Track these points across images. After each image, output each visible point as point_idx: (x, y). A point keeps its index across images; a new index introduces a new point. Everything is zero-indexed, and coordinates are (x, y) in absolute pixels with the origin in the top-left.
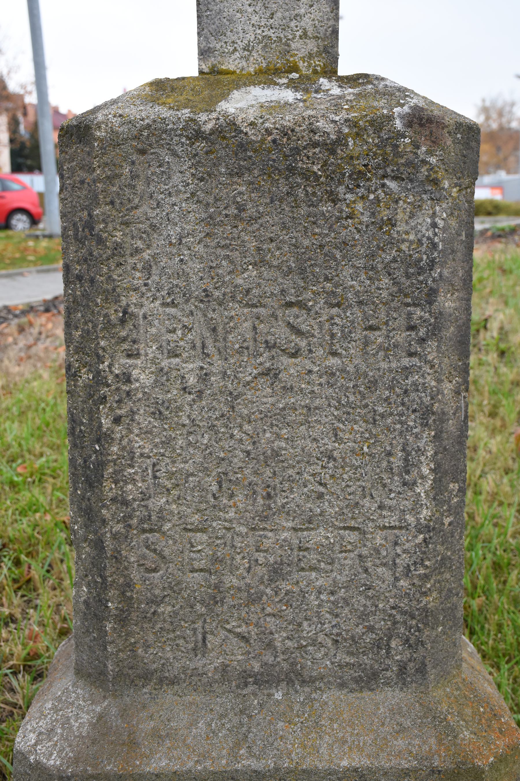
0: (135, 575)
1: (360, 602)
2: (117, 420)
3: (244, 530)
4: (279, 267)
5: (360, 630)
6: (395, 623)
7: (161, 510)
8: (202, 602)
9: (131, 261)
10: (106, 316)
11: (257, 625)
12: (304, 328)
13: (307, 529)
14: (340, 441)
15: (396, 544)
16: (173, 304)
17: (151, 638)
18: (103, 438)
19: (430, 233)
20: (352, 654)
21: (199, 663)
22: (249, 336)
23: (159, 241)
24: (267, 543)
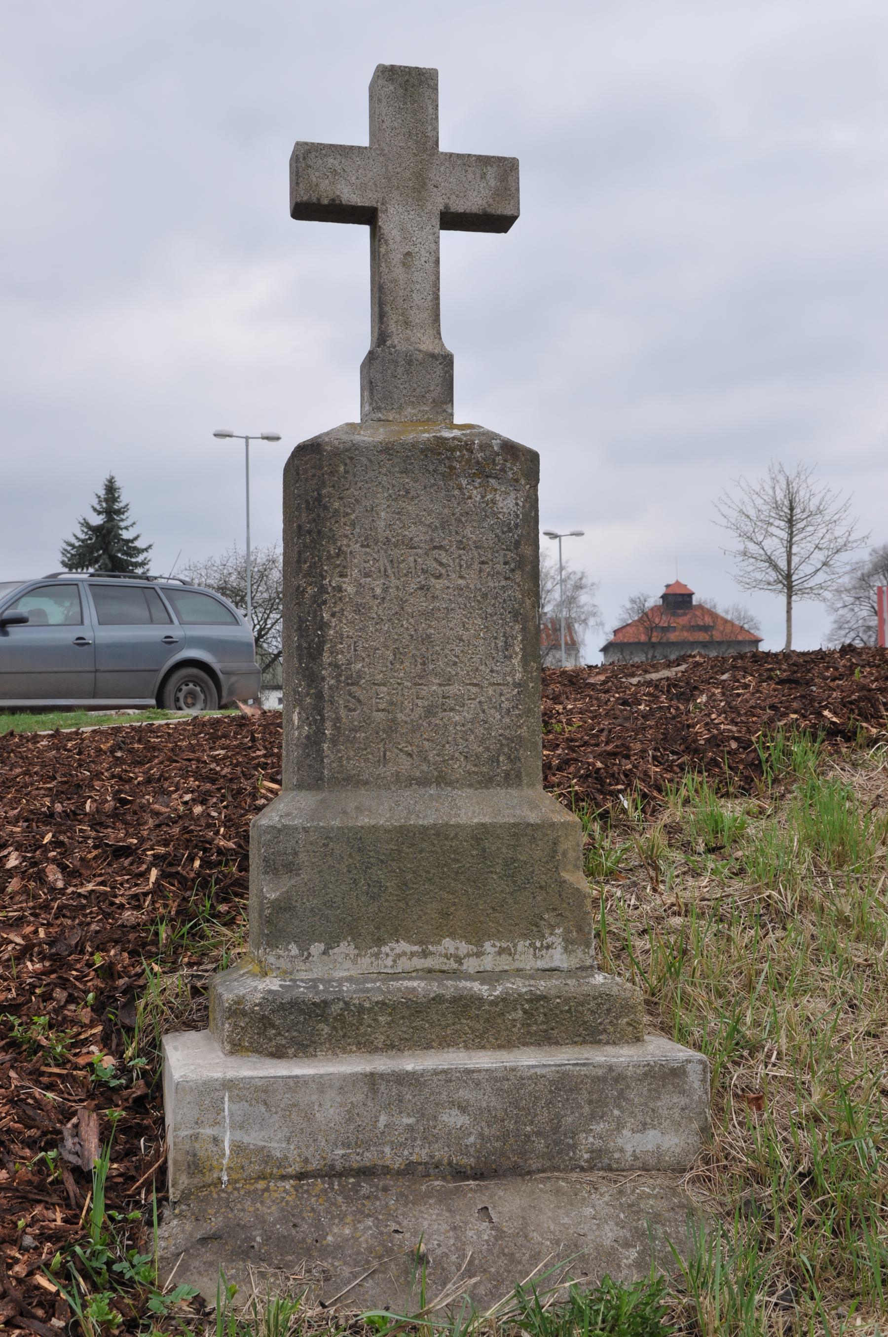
0: (343, 713)
1: (480, 731)
2: (333, 615)
3: (409, 684)
4: (429, 526)
5: (481, 749)
6: (502, 745)
7: (359, 671)
8: (384, 731)
10: (328, 551)
11: (418, 746)
12: (444, 561)
14: (468, 630)
15: (501, 694)
16: (368, 546)
17: (352, 753)
18: (323, 625)
20: (475, 765)
21: (381, 770)
22: (412, 565)
23: (359, 509)
24: (423, 693)
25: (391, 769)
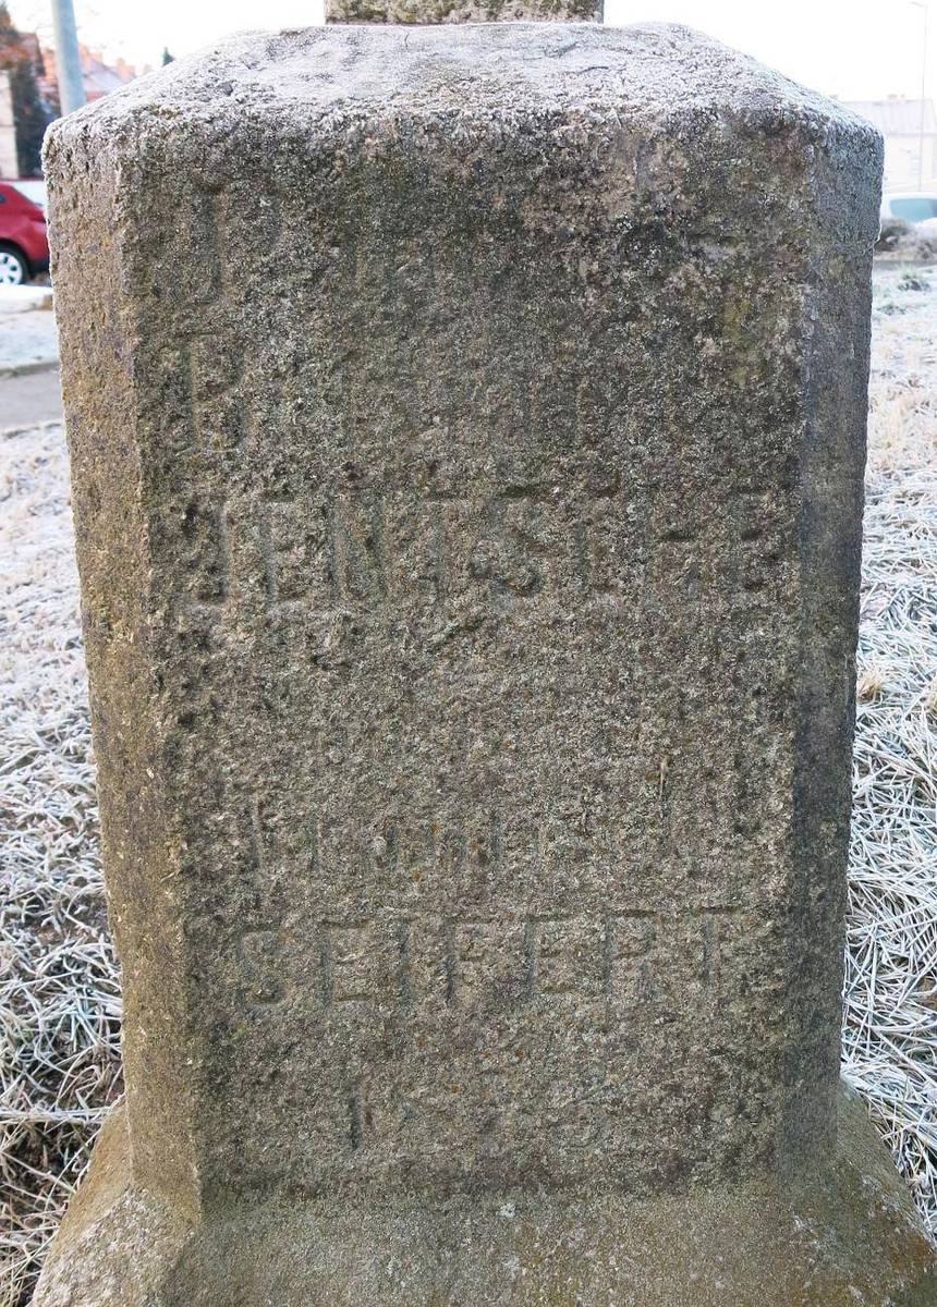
1: (654, 1042)
5: (656, 1092)
6: (720, 1078)
7: (279, 888)
9: (200, 409)
13: (556, 917)
19: (789, 349)
25: (381, 1156)
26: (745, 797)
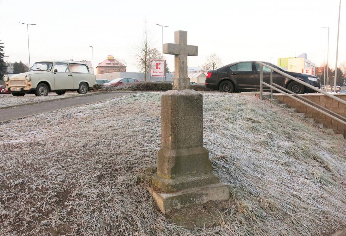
25: (185, 146)
26: (200, 126)
